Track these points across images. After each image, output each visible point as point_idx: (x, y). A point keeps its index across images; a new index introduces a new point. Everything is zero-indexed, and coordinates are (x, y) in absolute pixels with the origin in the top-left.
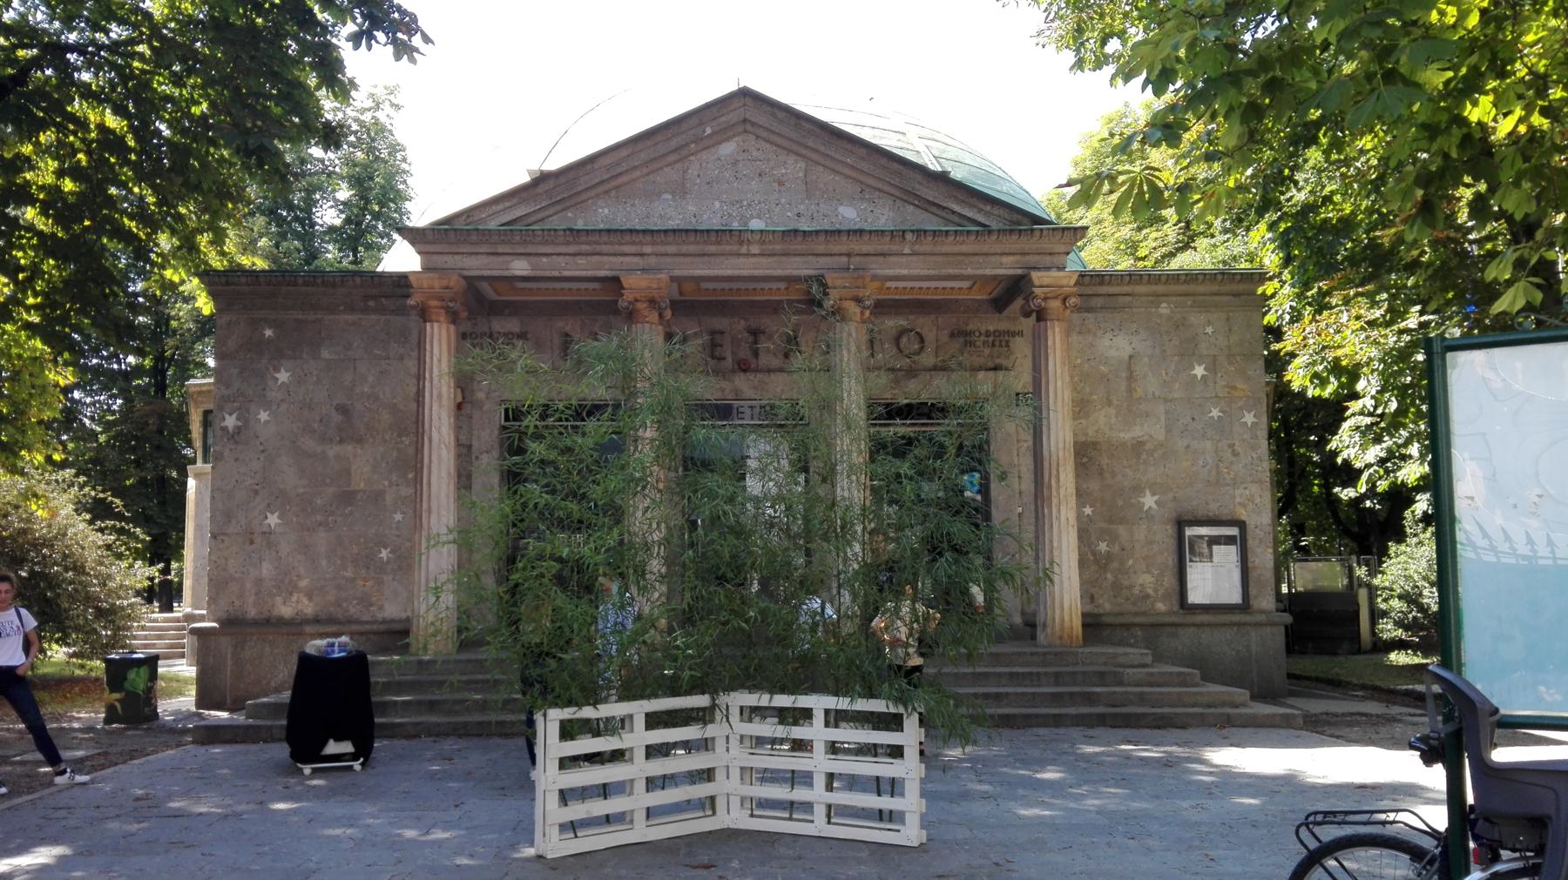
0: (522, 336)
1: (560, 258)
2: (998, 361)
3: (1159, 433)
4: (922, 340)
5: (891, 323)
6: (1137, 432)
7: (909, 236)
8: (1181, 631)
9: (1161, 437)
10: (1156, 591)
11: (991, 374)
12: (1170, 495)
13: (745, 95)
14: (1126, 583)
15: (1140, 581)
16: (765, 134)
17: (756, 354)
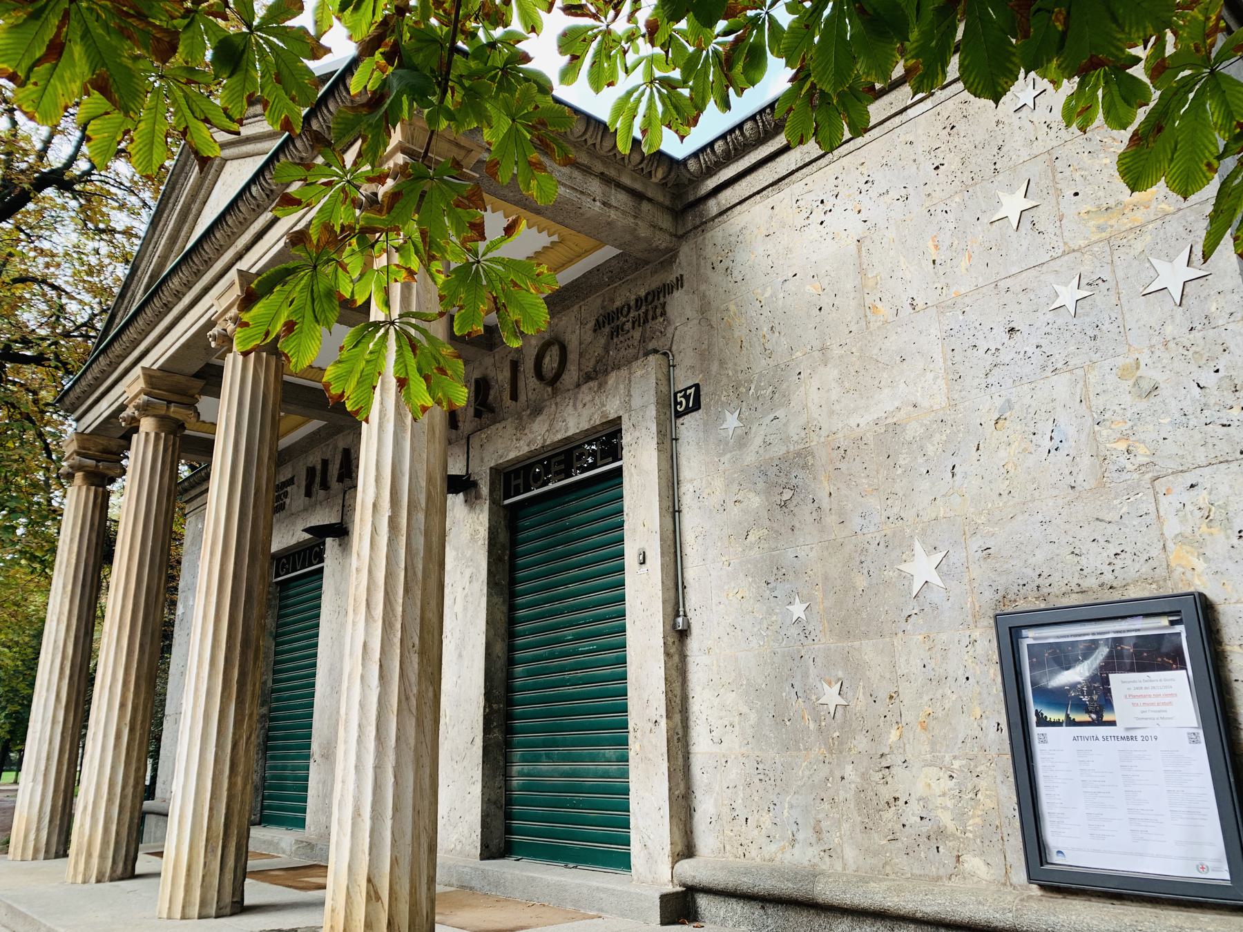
3: (931, 391)
6: (884, 403)
9: (940, 401)
10: (961, 817)
12: (976, 544)
14: (886, 793)
15: (920, 789)
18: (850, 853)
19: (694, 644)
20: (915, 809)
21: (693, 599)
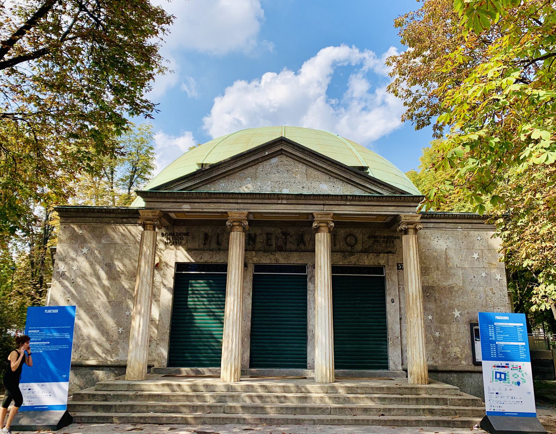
0: (187, 234)
1: (203, 204)
2: (389, 249)
4: (356, 240)
5: (342, 232)
6: (450, 282)
7: (349, 197)
8: (474, 375)
10: (461, 355)
11: (386, 255)
12: (466, 311)
13: (282, 141)
14: (448, 351)
15: (454, 351)
16: (290, 155)
17: (286, 244)
18: (440, 362)
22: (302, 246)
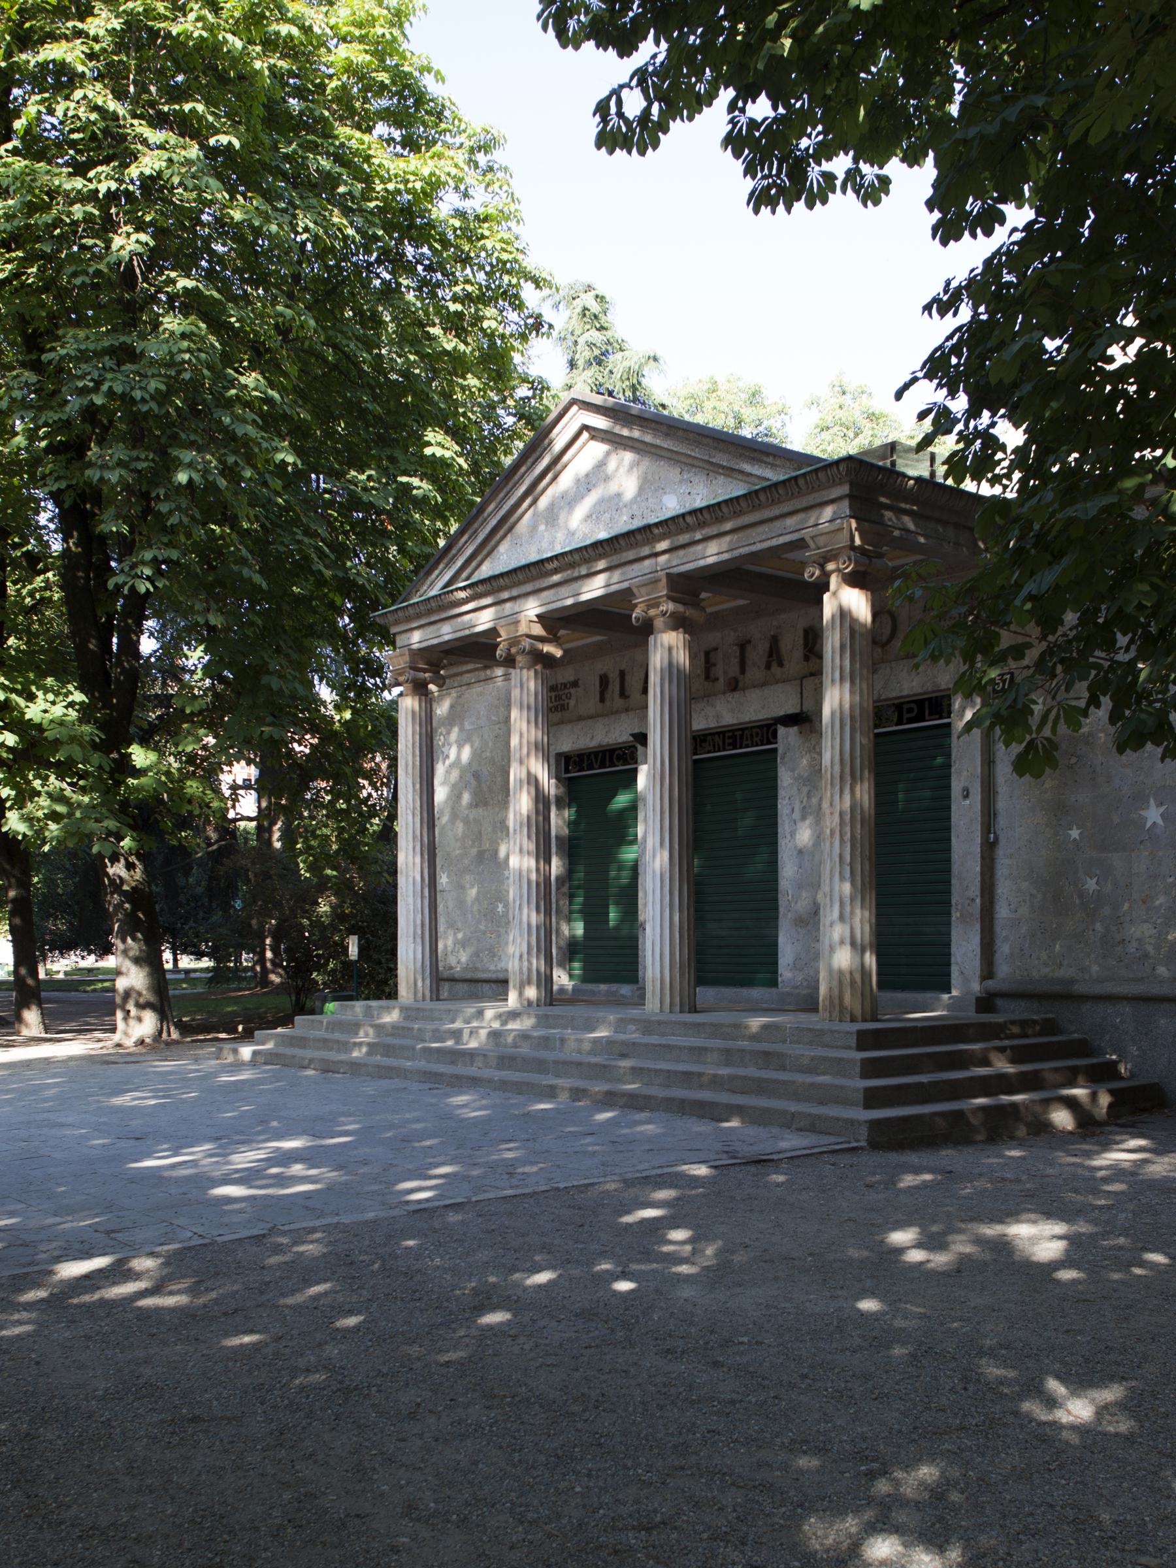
7: (689, 519)
10: (1157, 948)
18: (1095, 969)
19: (1000, 852)
20: (1134, 944)
21: (1002, 822)
22: (776, 670)
